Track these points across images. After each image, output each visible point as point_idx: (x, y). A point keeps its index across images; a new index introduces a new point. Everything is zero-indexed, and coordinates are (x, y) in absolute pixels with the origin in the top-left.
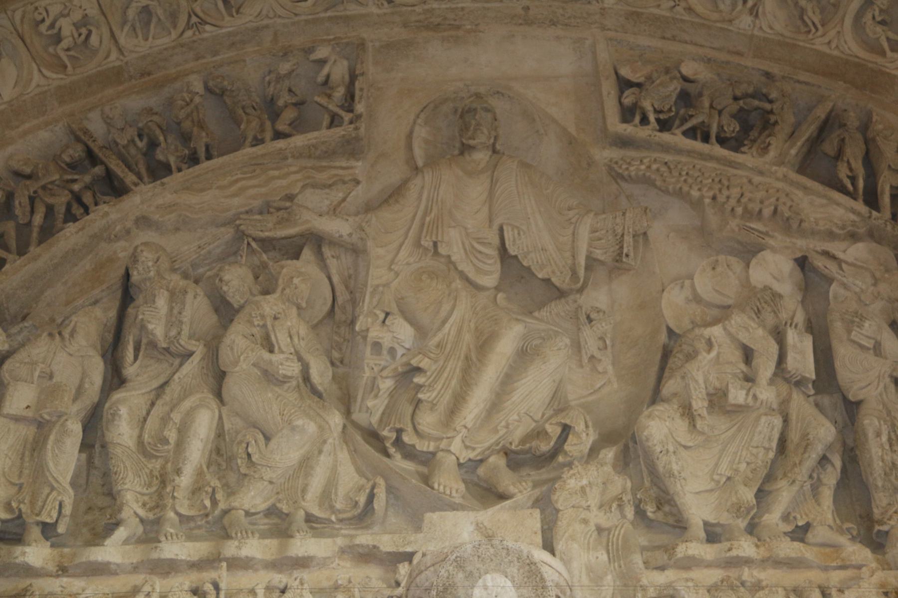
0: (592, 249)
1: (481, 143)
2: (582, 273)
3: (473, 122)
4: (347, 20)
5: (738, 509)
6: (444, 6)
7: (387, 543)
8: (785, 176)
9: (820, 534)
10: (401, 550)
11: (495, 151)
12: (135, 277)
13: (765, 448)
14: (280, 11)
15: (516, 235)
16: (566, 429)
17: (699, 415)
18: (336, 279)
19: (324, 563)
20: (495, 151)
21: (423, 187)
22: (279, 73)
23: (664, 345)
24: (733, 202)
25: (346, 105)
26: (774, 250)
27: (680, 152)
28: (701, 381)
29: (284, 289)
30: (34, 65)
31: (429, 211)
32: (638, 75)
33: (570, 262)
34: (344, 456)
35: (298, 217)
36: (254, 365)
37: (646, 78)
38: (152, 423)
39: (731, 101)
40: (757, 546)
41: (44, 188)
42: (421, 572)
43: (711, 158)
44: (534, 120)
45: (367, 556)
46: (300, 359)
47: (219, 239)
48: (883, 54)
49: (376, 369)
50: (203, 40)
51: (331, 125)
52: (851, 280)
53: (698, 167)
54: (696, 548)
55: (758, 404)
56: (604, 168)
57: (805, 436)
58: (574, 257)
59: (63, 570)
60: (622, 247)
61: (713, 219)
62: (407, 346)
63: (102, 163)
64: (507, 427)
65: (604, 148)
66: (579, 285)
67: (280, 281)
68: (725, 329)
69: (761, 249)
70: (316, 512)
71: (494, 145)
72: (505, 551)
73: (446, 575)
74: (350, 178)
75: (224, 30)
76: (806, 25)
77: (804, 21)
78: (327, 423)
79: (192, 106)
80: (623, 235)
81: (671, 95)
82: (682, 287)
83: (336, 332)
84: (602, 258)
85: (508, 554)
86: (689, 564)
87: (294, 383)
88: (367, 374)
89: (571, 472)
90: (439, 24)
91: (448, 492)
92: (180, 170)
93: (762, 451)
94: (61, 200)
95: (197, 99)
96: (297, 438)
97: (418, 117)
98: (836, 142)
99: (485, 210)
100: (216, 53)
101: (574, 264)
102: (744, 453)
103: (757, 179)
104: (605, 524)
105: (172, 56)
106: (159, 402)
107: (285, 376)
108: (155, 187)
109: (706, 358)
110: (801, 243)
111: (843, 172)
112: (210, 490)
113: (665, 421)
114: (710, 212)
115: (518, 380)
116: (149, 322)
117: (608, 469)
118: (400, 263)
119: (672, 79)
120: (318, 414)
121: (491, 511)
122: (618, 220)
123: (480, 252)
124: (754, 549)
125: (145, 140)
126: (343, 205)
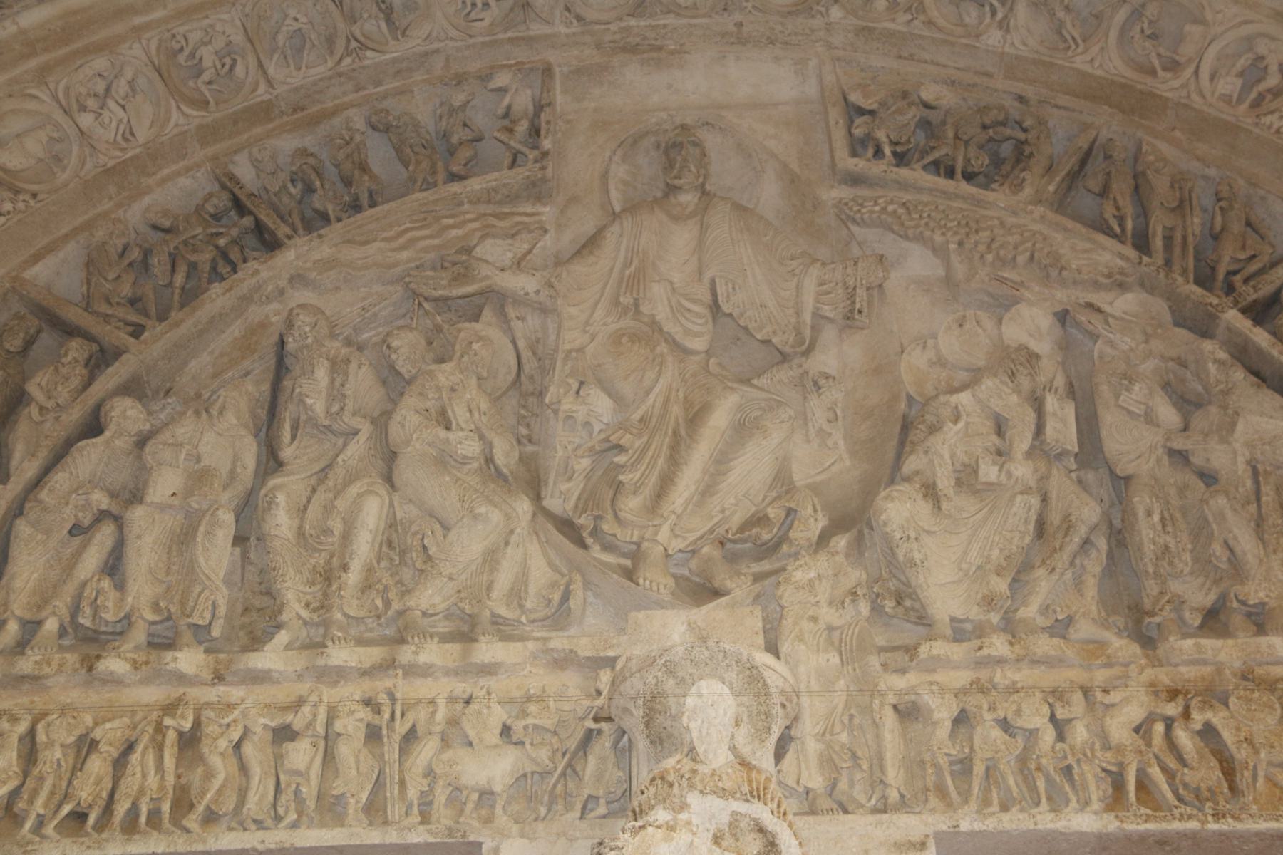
0: (818, 305)
2: (807, 332)
3: (679, 158)
4: (530, 41)
5: (989, 602)
6: (642, 23)
9: (1085, 629)
10: (602, 654)
11: (704, 193)
12: (291, 345)
13: (1020, 532)
14: (453, 33)
15: (731, 290)
17: (945, 495)
20: (704, 193)
21: (621, 236)
22: (452, 105)
27: (920, 190)
28: (947, 456)
30: (173, 102)
32: (870, 101)
34: (534, 548)
35: (476, 273)
37: (880, 104)
38: (314, 511)
39: (979, 130)
40: (1011, 644)
41: (185, 243)
42: (625, 679)
43: (957, 196)
44: (750, 156)
45: (563, 662)
48: (1153, 72)
50: (363, 67)
51: (513, 164)
52: (1118, 336)
53: (941, 208)
55: (1012, 481)
57: (1066, 517)
59: (219, 678)
60: (854, 302)
61: (960, 269)
62: (605, 421)
63: (251, 213)
64: (723, 511)
65: (832, 187)
66: (804, 347)
67: (457, 347)
69: (1016, 301)
70: (503, 611)
72: (722, 654)
73: (654, 682)
75: (388, 56)
76: (1065, 41)
77: (1062, 36)
78: (515, 510)
79: (353, 145)
80: (855, 288)
82: (924, 348)
84: (831, 315)
85: (725, 657)
88: (560, 453)
89: (797, 563)
90: (637, 45)
91: (655, 588)
92: (339, 220)
94: (205, 257)
95: (358, 138)
96: (480, 527)
97: (614, 153)
100: (378, 83)
102: (997, 538)
103: (1011, 220)
105: (328, 87)
106: (321, 489)
107: (465, 457)
108: (311, 240)
109: (952, 431)
110: (1062, 296)
111: (1109, 212)
113: (906, 502)
115: (735, 459)
116: (307, 396)
117: (840, 558)
121: (705, 609)
122: (849, 271)
123: (689, 310)
124: (1009, 647)
125: (300, 185)
126: (528, 258)
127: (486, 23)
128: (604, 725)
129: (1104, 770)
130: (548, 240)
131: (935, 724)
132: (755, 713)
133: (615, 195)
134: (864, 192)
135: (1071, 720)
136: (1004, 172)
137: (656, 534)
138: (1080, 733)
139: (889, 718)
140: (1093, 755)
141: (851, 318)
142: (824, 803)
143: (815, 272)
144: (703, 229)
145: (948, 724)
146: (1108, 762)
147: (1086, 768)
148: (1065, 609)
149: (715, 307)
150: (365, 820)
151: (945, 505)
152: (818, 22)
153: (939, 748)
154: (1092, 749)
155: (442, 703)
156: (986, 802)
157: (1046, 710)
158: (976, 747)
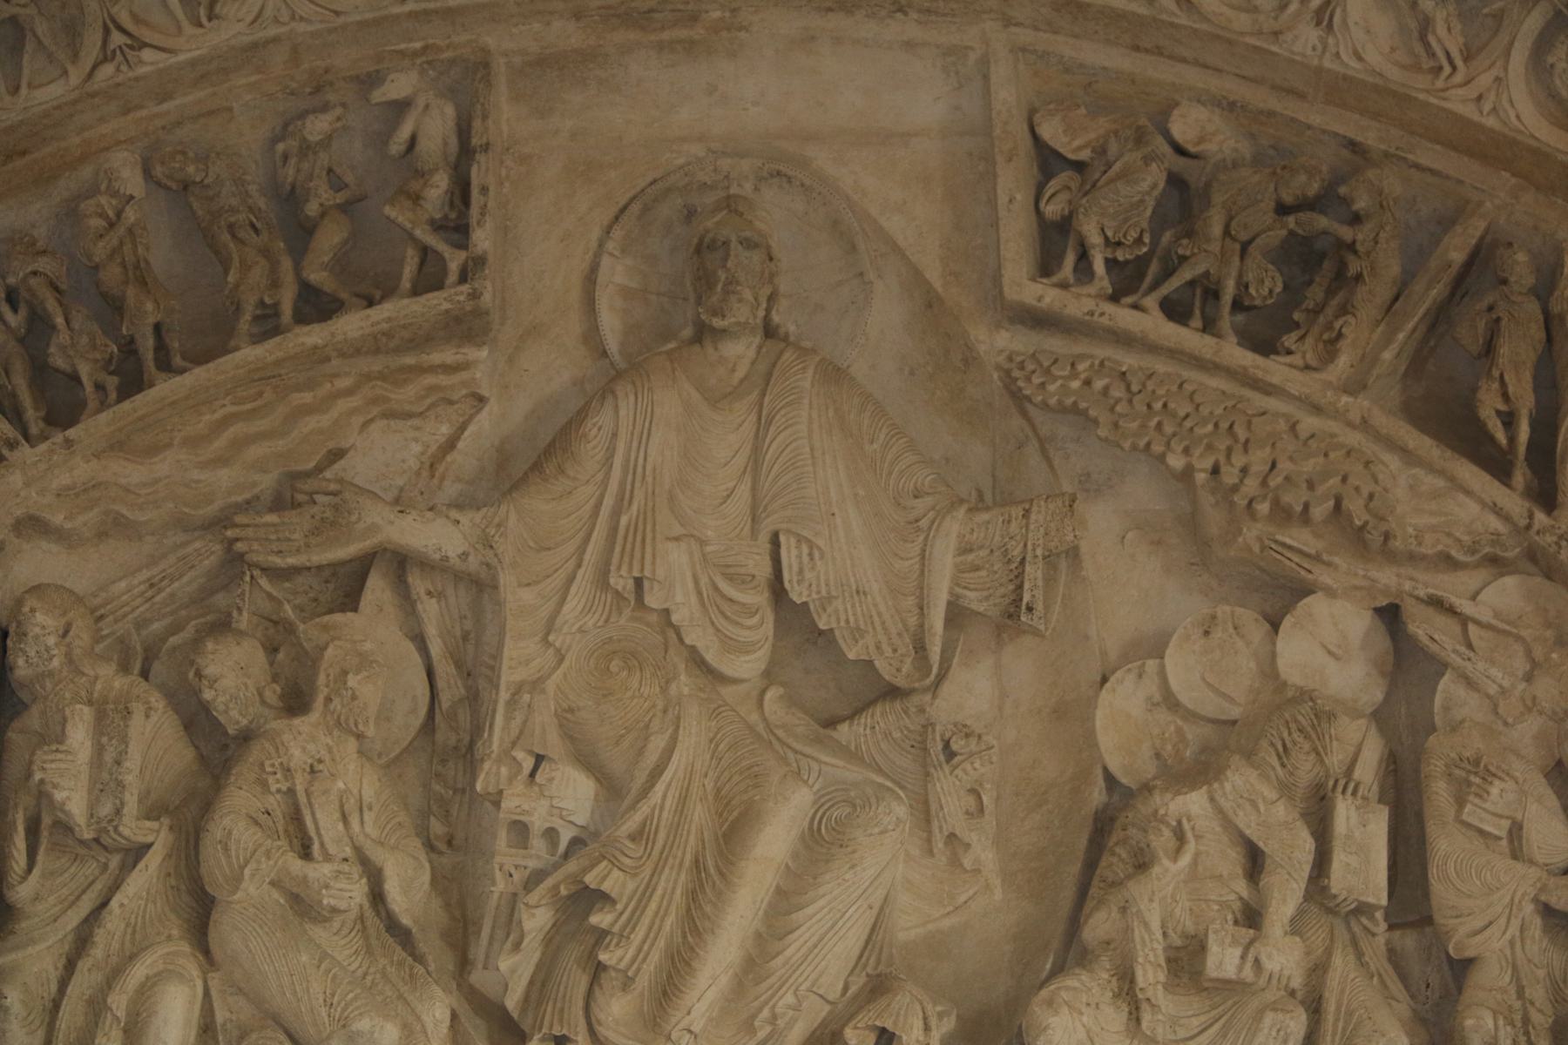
0: (958, 590)
1: (738, 324)
3: (722, 275)
8: (1364, 421)
11: (770, 331)
15: (806, 558)
18: (436, 648)
20: (770, 331)
21: (615, 435)
22: (305, 139)
23: (1096, 813)
24: (1251, 486)
25: (453, 215)
26: (1330, 593)
27: (1153, 348)
28: (1155, 925)
29: (328, 700)
31: (626, 503)
32: (1076, 143)
33: (913, 621)
35: (354, 518)
36: (273, 883)
39: (1270, 217)
43: (1214, 368)
47: (193, 567)
49: (516, 876)
50: (137, 79)
52: (1481, 666)
53: (1188, 387)
55: (1262, 982)
56: (995, 376)
58: (921, 608)
60: (1020, 587)
61: (1214, 518)
64: (774, 1017)
65: (998, 326)
66: (928, 682)
68: (1212, 799)
69: (1304, 590)
71: (767, 319)
74: (464, 392)
77: (1427, 46)
78: (419, 1018)
79: (121, 230)
80: (1023, 562)
81: (1142, 201)
82: (1140, 676)
83: (438, 775)
87: (353, 915)
88: (500, 886)
90: (651, 11)
92: (103, 406)
95: (131, 215)
97: (608, 231)
98: (1481, 325)
99: (744, 490)
100: (166, 97)
101: (922, 626)
103: (1309, 423)
105: (72, 115)
106: (83, 965)
108: (52, 451)
109: (1169, 871)
110: (1387, 577)
111: (1489, 407)
114: (1207, 499)
116: (55, 786)
118: (565, 629)
119: (1147, 160)
120: (400, 997)
125: (23, 311)
126: (449, 458)
133: (610, 323)
134: (1056, 344)
136: (1310, 304)
143: (954, 527)
144: (763, 425)
151: (1146, 1017)
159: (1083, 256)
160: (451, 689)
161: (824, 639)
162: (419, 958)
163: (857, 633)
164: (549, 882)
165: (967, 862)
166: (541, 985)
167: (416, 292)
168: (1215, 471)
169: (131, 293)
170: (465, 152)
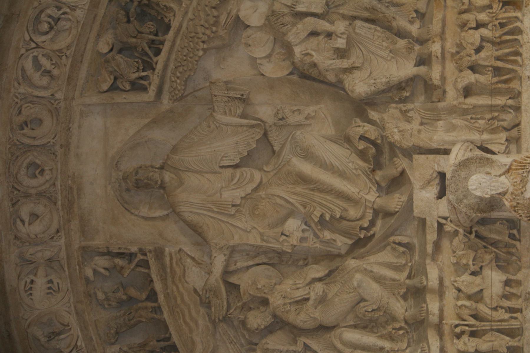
0: (237, 115)
1: (160, 177)
3: (146, 181)
4: (68, 258)
5: (410, 49)
7: (431, 236)
10: (436, 229)
13: (374, 32)
15: (227, 158)
16: (362, 138)
17: (352, 64)
18: (251, 263)
19: (441, 270)
20: (162, 168)
21: (191, 212)
22: (104, 299)
23: (300, 78)
24: (208, 32)
25: (127, 257)
26: (238, 10)
27: (168, 59)
29: (265, 293)
31: (211, 209)
32: (109, 79)
33: (245, 128)
34: (372, 259)
35: (213, 286)
36: (316, 309)
37: (111, 75)
40: (434, 42)
42: (459, 221)
45: (437, 246)
46: (310, 283)
47: (226, 331)
49: (315, 240)
50: (86, 347)
53: (180, 49)
54: (435, 74)
56: (176, 104)
57: (367, 9)
58: (242, 126)
60: (236, 98)
61: (217, 43)
62: (300, 223)
64: (356, 169)
65: (161, 103)
66: (262, 124)
67: (259, 295)
68: (296, 45)
69: (238, 17)
70: (406, 274)
71: (158, 168)
72: (453, 178)
73: (465, 209)
74: (178, 255)
80: (228, 97)
81: (126, 61)
82: (261, 65)
83: (286, 263)
85: (454, 177)
86: (443, 78)
87: (325, 286)
88: (317, 245)
89: (390, 137)
90: (68, 200)
91: (401, 203)
93: (376, 33)
96: (364, 284)
97: (132, 213)
99: (207, 176)
100: (91, 339)
101: (246, 126)
102: (377, 43)
103: (190, 15)
104: (419, 120)
109: (316, 58)
112: (394, 331)
113: (355, 83)
114: (212, 45)
115: (325, 161)
117: (386, 116)
118: (246, 226)
119: (114, 59)
120: (348, 273)
122: (219, 99)
123: (239, 180)
124: (436, 44)
126: (197, 259)
127: (59, 281)
128: (474, 230)
129: (501, 9)
130: (186, 249)
131: (476, 81)
132: (480, 165)
133: (159, 213)
134: (166, 87)
135: (476, 21)
136: (156, 14)
137: (370, 202)
138: (483, 17)
139: (472, 101)
140: (495, 13)
141: (244, 100)
142: (514, 133)
143: (219, 116)
145: (477, 75)
146: (498, 6)
147: (500, 16)
148: (411, 13)
149: (236, 166)
150: (519, 337)
151: (357, 65)
152: (62, 105)
153: (489, 81)
154: (492, 13)
155: (460, 303)
156: (515, 62)
157: (472, 31)
158: (489, 64)
159: (141, 78)
160: (262, 259)
161: (250, 154)
162: (337, 268)
163: (249, 144)
164: (317, 231)
165: (313, 114)
166: (345, 233)
167: (149, 268)
168: (204, 42)
169: (147, 349)
170: (109, 253)
